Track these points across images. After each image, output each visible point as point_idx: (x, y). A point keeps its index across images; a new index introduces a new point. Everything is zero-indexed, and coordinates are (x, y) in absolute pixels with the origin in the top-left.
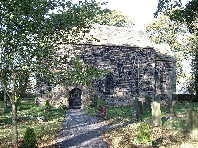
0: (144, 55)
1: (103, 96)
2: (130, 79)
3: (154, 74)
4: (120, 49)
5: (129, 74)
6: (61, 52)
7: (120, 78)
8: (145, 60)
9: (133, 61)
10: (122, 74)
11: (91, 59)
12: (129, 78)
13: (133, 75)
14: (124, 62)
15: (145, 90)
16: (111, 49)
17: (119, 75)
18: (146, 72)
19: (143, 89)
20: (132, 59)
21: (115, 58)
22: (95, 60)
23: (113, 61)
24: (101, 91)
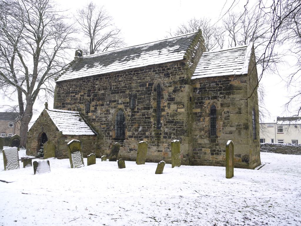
2: (146, 118)
5: (145, 108)
6: (72, 90)
7: (133, 115)
8: (170, 83)
9: (152, 88)
10: (136, 110)
11: (99, 94)
12: (144, 115)
13: (151, 110)
14: (138, 91)
16: (121, 76)
18: (172, 103)
19: (166, 133)
20: (150, 85)
21: (126, 87)
22: (103, 94)
23: (124, 92)
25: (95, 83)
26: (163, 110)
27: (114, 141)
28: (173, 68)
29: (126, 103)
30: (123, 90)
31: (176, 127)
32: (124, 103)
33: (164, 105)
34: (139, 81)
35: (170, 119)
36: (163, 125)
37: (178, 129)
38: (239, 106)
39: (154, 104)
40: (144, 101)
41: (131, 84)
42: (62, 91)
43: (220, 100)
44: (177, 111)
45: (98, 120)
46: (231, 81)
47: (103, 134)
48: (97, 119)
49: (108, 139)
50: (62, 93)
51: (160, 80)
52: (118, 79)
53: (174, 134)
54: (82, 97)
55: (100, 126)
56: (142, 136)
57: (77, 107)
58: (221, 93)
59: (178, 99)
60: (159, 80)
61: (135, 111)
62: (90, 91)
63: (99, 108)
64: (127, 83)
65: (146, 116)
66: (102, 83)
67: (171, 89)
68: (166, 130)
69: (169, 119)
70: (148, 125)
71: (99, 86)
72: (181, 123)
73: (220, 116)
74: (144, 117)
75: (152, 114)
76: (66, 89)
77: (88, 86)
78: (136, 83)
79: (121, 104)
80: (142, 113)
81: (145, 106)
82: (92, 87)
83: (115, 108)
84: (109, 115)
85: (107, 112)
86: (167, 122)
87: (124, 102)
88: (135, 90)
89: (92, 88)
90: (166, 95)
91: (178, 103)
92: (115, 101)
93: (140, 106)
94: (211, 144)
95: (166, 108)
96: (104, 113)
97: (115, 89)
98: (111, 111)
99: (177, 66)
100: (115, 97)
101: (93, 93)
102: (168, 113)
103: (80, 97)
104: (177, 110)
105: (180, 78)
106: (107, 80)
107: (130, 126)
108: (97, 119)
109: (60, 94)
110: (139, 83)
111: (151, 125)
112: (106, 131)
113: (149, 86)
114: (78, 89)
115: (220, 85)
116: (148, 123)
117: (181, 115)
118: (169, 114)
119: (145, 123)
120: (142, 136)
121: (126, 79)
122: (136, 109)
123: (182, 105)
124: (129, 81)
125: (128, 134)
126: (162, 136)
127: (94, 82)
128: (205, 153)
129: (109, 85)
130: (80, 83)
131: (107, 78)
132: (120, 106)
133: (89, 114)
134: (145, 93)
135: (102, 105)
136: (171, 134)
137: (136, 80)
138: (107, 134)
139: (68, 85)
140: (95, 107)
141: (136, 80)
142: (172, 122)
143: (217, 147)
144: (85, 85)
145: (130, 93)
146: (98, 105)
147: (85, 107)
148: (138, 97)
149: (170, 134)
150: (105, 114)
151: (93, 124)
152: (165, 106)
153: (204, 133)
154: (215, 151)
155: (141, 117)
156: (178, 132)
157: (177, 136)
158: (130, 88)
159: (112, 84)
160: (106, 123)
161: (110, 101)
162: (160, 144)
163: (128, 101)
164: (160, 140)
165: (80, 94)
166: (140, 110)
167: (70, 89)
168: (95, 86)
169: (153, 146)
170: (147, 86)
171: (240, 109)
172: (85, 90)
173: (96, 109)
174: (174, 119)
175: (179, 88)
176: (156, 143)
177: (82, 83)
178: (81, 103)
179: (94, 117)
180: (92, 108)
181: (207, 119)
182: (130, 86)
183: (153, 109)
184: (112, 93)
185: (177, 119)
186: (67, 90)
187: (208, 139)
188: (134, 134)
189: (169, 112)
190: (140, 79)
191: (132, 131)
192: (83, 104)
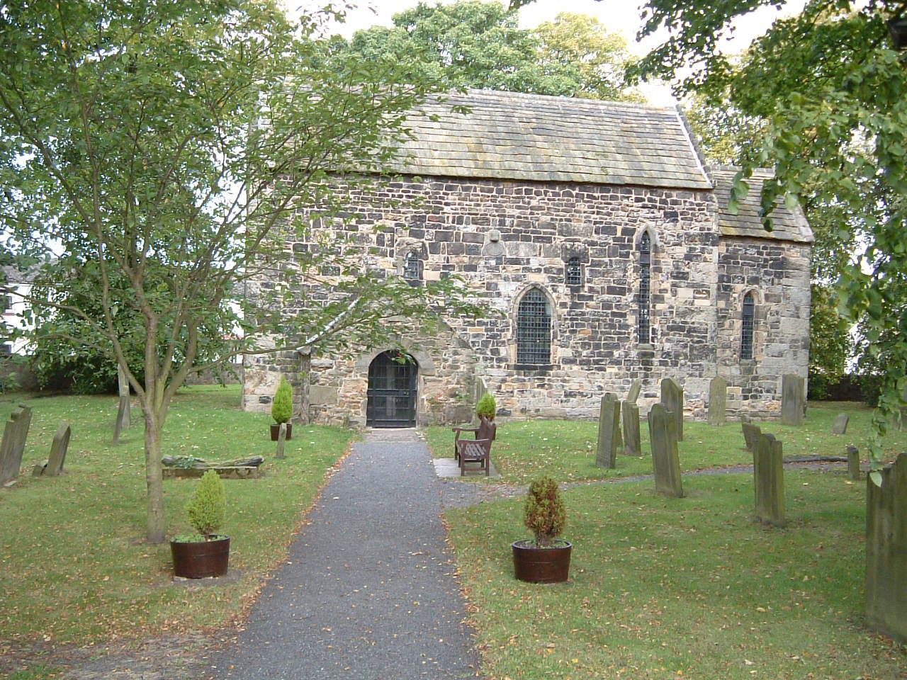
1: (504, 381)
2: (614, 314)
3: (714, 292)
4: (574, 193)
5: (611, 290)
7: (574, 306)
8: (679, 236)
10: (585, 291)
12: (610, 307)
13: (629, 297)
14: (593, 244)
16: (538, 194)
17: (573, 296)
18: (682, 285)
19: (668, 354)
20: (625, 232)
22: (474, 236)
23: (549, 240)
24: (499, 360)
25: (440, 198)
27: (515, 372)
28: (685, 202)
29: (555, 271)
30: (545, 233)
31: (689, 339)
32: (547, 271)
33: (662, 287)
34: (595, 216)
36: (659, 333)
37: (696, 345)
38: (796, 303)
39: (634, 281)
40: (607, 272)
41: (570, 221)
43: (764, 286)
44: (692, 304)
46: (783, 249)
49: (492, 367)
51: (653, 224)
52: (527, 200)
53: (686, 357)
54: (388, 236)
55: (465, 330)
56: (602, 361)
59: (696, 277)
60: (648, 221)
61: (583, 296)
62: (422, 219)
64: (557, 215)
65: (614, 310)
66: (468, 203)
67: (681, 251)
68: (667, 346)
69: (673, 322)
70: (620, 333)
71: (459, 211)
72: (702, 333)
73: (762, 321)
74: (610, 311)
79: (539, 270)
81: (612, 285)
83: (516, 279)
84: (496, 300)
85: (487, 289)
87: (548, 266)
88: (583, 239)
89: (428, 213)
90: (667, 265)
91: (699, 288)
92: (516, 261)
93: (598, 283)
94: (743, 377)
97: (518, 226)
100: (517, 249)
101: (434, 227)
102: (671, 307)
107: (568, 334)
111: (629, 333)
112: (485, 344)
113: (622, 234)
115: (765, 256)
116: (620, 327)
117: (703, 314)
119: (612, 326)
121: (554, 204)
122: (586, 289)
125: (558, 352)
126: (656, 360)
127: (439, 193)
128: (732, 397)
129: (496, 211)
132: (534, 278)
134: (611, 252)
135: (472, 268)
136: (679, 355)
137: (585, 212)
138: (489, 353)
140: (442, 271)
141: (585, 212)
144: (401, 196)
145: (569, 247)
146: (454, 266)
148: (590, 259)
149: (677, 356)
152: (666, 290)
153: (731, 354)
154: (750, 391)
155: (601, 310)
156: (695, 352)
157: (691, 360)
159: (507, 210)
161: (499, 259)
162: (650, 380)
163: (560, 267)
164: (651, 369)
166: (598, 292)
168: (442, 209)
170: (619, 234)
171: (797, 308)
172: (400, 212)
174: (686, 323)
178: (384, 255)
180: (430, 275)
181: (738, 324)
182: (566, 225)
183: (633, 294)
184: (506, 238)
185: (693, 323)
187: (737, 366)
190: (598, 213)
192: (391, 256)
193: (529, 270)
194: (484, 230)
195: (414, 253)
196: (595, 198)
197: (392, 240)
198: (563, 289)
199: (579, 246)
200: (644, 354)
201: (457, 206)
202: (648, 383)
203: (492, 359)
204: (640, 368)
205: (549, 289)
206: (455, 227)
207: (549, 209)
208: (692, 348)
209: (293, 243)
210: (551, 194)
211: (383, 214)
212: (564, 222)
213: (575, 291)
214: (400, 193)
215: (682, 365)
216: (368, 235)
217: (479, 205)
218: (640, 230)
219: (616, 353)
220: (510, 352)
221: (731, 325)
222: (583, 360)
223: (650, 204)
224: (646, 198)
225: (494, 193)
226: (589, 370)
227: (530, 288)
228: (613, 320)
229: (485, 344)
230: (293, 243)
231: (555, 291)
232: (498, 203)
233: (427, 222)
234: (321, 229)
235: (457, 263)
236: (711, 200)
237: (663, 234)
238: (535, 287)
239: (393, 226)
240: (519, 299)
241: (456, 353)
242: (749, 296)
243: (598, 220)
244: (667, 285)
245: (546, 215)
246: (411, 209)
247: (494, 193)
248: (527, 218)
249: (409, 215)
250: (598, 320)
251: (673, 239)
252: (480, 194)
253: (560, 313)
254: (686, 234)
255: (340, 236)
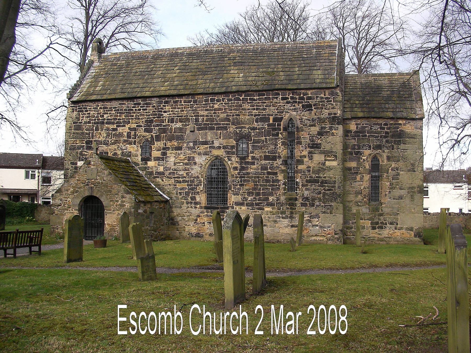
0: (310, 106)
1: (199, 216)
2: (269, 173)
3: (339, 155)
5: (266, 158)
6: (110, 118)
7: (242, 168)
8: (313, 120)
9: (279, 125)
11: (171, 129)
12: (266, 169)
13: (279, 162)
14: (254, 129)
15: (314, 200)
16: (218, 101)
17: (241, 163)
18: (317, 152)
19: (307, 199)
20: (275, 120)
21: (229, 120)
22: (180, 129)
23: (226, 128)
24: (196, 203)
25: (161, 108)
26: (300, 162)
28: (317, 97)
31: (322, 188)
32: (224, 147)
34: (255, 111)
35: (314, 176)
36: (300, 184)
37: (327, 192)
39: (282, 151)
40: (264, 146)
41: (239, 115)
42: (85, 119)
44: (324, 164)
45: (170, 174)
46: (401, 124)
47: (181, 199)
48: (167, 173)
49: (191, 207)
50: (86, 123)
51: (295, 113)
53: (320, 200)
54: (133, 133)
56: (261, 203)
57: (122, 149)
58: (387, 141)
61: (248, 162)
62: (151, 121)
63: (171, 153)
64: (232, 113)
65: (269, 170)
66: (177, 110)
67: (315, 130)
68: (306, 193)
69: (310, 177)
70: (273, 185)
71: (172, 116)
72: (332, 183)
73: (385, 174)
75: (281, 168)
76: (96, 116)
77: (146, 112)
78: (248, 116)
79: (219, 148)
80: (261, 165)
82: (156, 114)
83: (206, 154)
84: (194, 167)
86: (307, 181)
87: (225, 144)
88: (247, 126)
89: (155, 118)
91: (327, 153)
94: (371, 214)
95: (306, 159)
96: (183, 163)
97: (207, 121)
98: (197, 160)
99: (325, 95)
101: (158, 125)
102: (309, 167)
103: (129, 131)
104: (325, 163)
105: (329, 114)
106: (189, 105)
107: (238, 187)
108: (167, 173)
109: (80, 123)
110: (255, 116)
111: (279, 185)
112: (187, 194)
114: (124, 117)
117: (332, 171)
118: (311, 169)
119: (268, 181)
120: (261, 203)
122: (250, 158)
123: (334, 155)
124: (233, 111)
126: (298, 203)
128: (363, 228)
130: (128, 107)
131: (190, 102)
132: (216, 152)
133: (149, 162)
134: (266, 133)
135: (179, 148)
138: (190, 199)
139: (101, 108)
140: (162, 151)
142: (316, 181)
143: (382, 218)
144: (140, 110)
147: (140, 151)
148: (253, 138)
149: (314, 200)
150: (186, 164)
151: (159, 182)
152: (305, 156)
153: (362, 198)
154: (377, 223)
155: (260, 171)
158: (237, 123)
160: (187, 179)
161: (195, 143)
163: (233, 144)
165: (127, 126)
166: (258, 159)
167: (105, 116)
169: (283, 218)
170: (271, 121)
171: (413, 165)
172: (139, 119)
173: (164, 154)
174: (320, 177)
175: (327, 129)
176: (288, 213)
177: (133, 107)
178: (130, 143)
179: (161, 169)
180: (156, 154)
181: (367, 177)
183: (281, 160)
184: (199, 129)
185: (325, 177)
186: (97, 117)
187: (367, 206)
188: (246, 200)
189: (312, 165)
190: (257, 109)
191: (243, 195)
192: (135, 144)
193: (213, 148)
194: (186, 125)
195: (147, 140)
196: (254, 100)
197: (135, 135)
198: (234, 159)
199: (245, 131)
200: (290, 199)
201: (171, 113)
202: (293, 218)
203: (191, 203)
204: (288, 208)
205: (226, 159)
206: (169, 125)
207: (225, 109)
208: (324, 194)
209: (86, 140)
210: (226, 100)
211: (130, 120)
212: (235, 117)
213: (243, 159)
214: (140, 108)
215: (317, 206)
216: (122, 133)
217: (183, 111)
218: (286, 117)
219: (271, 199)
220: (202, 198)
221: (362, 178)
222: (249, 203)
223: (292, 101)
224: (289, 97)
225: (192, 103)
226: (253, 209)
227: (214, 158)
228: (268, 177)
229: (187, 194)
230: (86, 140)
231: (230, 160)
232: (194, 109)
233: (154, 123)
234: (99, 131)
235: (171, 146)
236: (337, 94)
237: (302, 119)
238: (217, 157)
239: (135, 127)
240: (207, 165)
241: (123, 197)
242: (375, 159)
243: (257, 114)
244: (305, 153)
245: (223, 113)
246: (145, 116)
247: (192, 103)
248: (212, 116)
249: (144, 120)
250: (258, 177)
251: (309, 122)
252: (184, 104)
253: (233, 173)
254: (318, 118)
255: (108, 135)
